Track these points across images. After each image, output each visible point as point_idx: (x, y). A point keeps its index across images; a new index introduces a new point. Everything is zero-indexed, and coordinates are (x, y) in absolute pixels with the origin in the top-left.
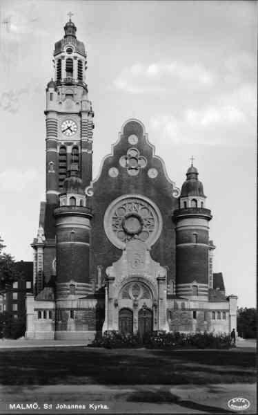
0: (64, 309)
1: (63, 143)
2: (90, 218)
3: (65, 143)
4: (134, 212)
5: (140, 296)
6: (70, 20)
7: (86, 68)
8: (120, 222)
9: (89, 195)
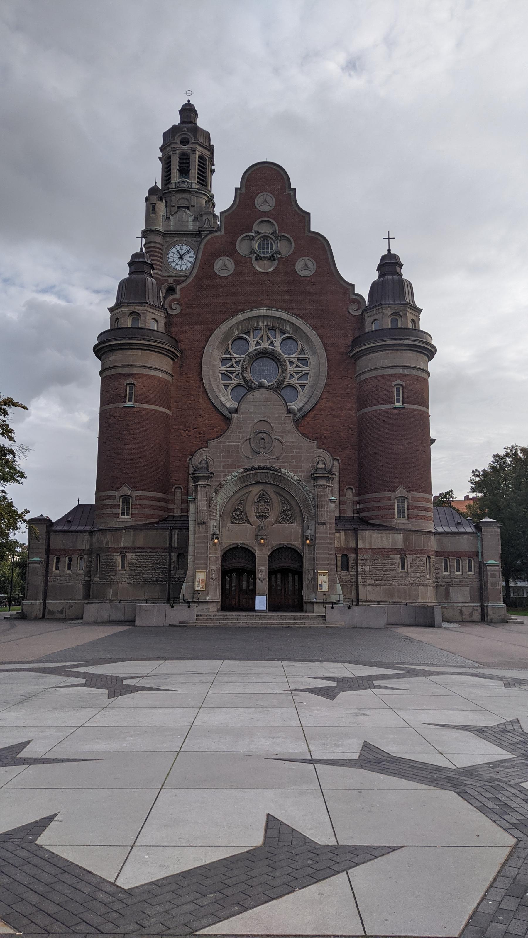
0: (110, 550)
1: (171, 280)
2: (173, 356)
3: (174, 281)
4: (265, 345)
5: (272, 519)
6: (189, 101)
7: (213, 171)
8: (238, 369)
9: (170, 312)
